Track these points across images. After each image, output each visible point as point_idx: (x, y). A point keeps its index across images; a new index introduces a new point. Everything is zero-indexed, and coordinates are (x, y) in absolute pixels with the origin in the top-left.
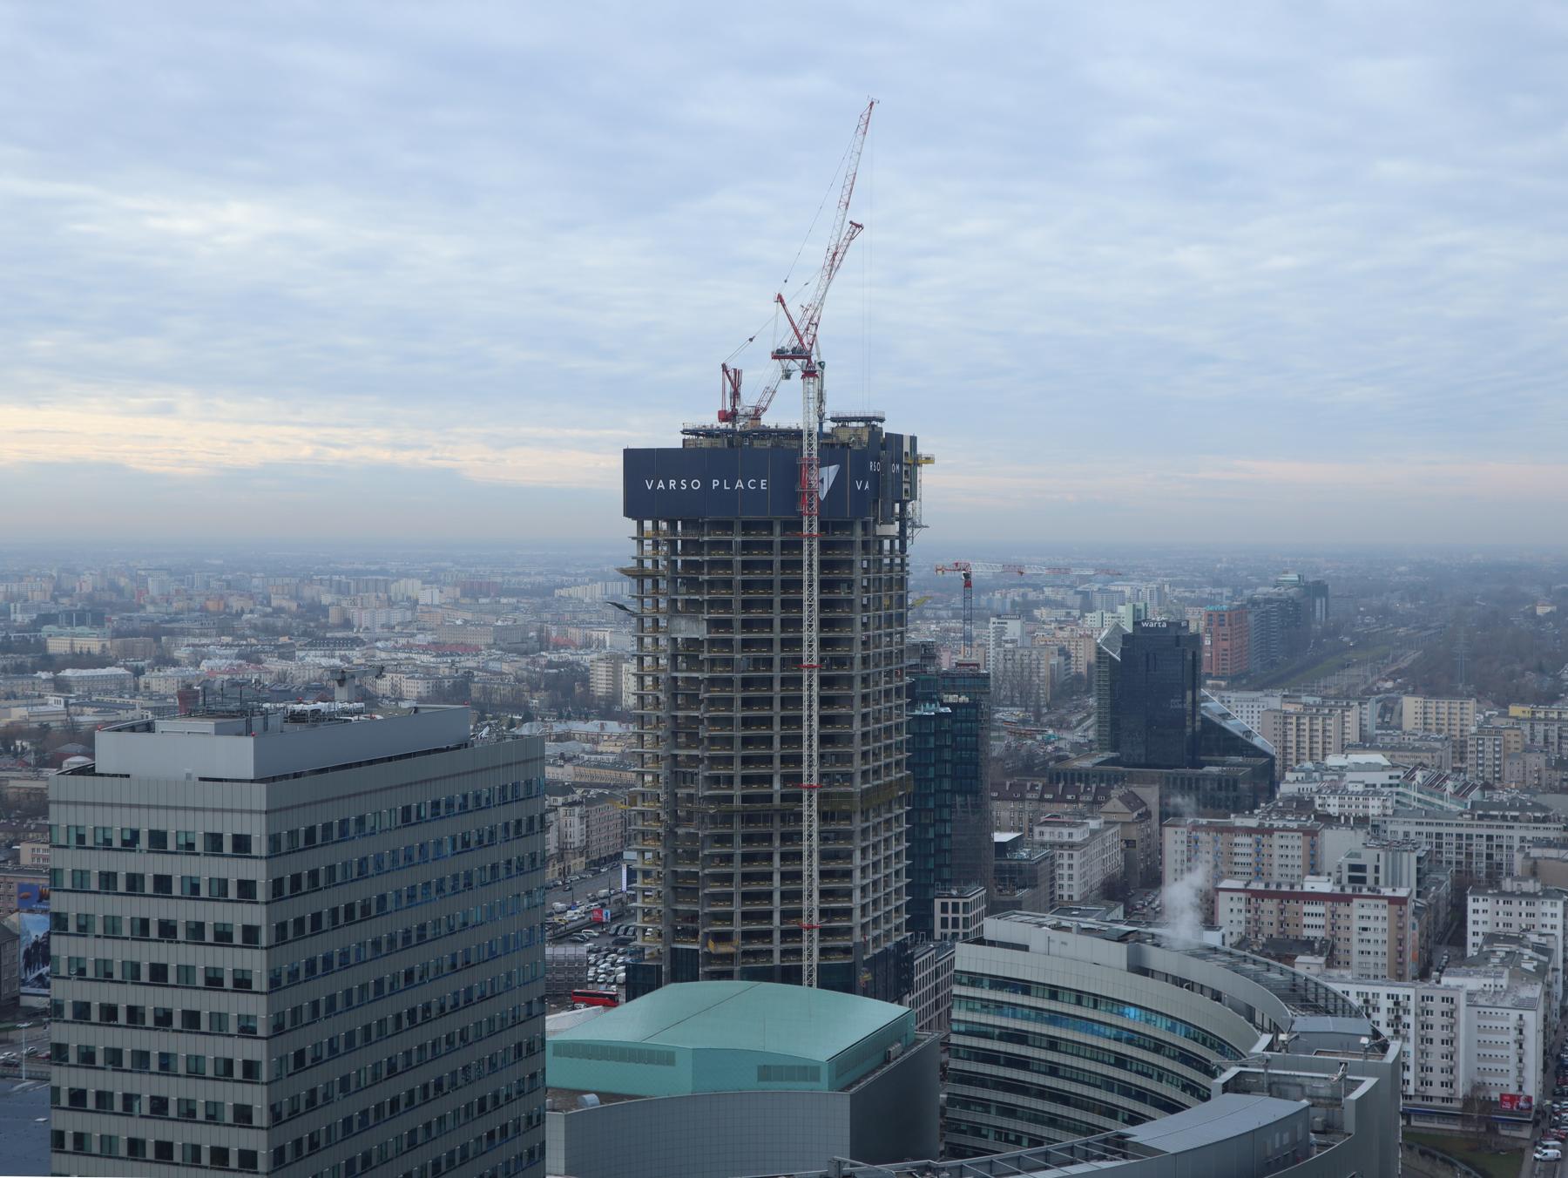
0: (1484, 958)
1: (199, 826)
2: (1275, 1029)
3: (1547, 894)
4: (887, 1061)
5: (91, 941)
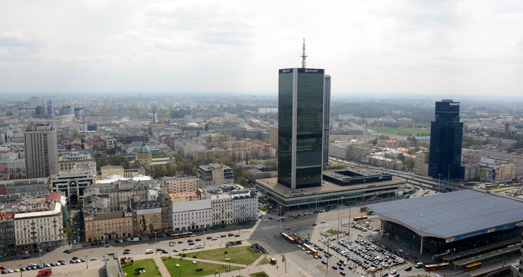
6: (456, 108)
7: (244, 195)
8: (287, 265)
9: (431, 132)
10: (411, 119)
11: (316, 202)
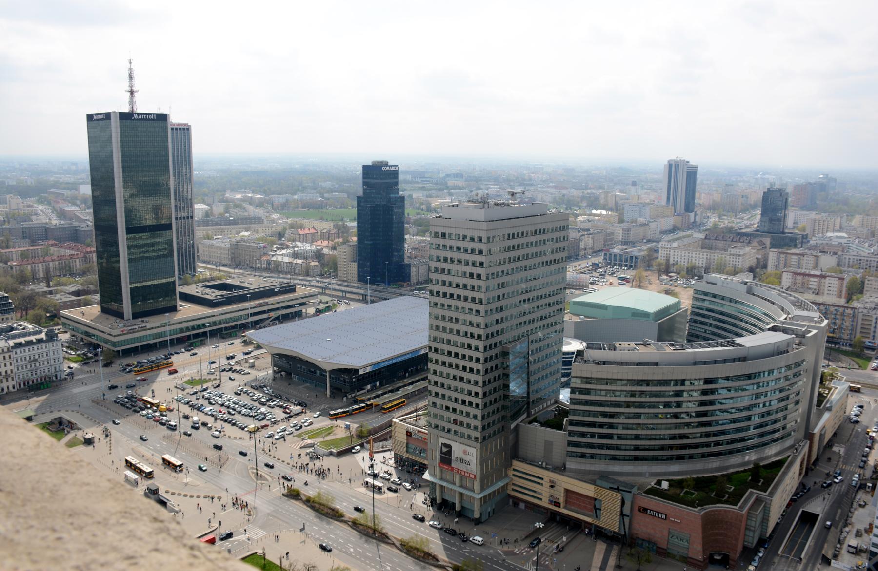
1: (469, 234)
7: (33, 338)
8: (113, 442)
9: (358, 214)
10: (345, 195)
11: (168, 338)
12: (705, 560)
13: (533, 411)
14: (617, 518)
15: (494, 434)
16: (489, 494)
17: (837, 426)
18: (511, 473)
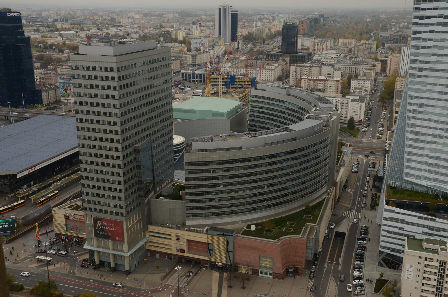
0: (354, 92)
1: (103, 65)
2: (316, 106)
3: (367, 80)
4: (237, 112)
5: (81, 89)
6: (18, 19)
12: (284, 272)
13: (158, 189)
14: (225, 254)
15: (134, 209)
16: (135, 252)
17: (347, 175)
18: (147, 234)
